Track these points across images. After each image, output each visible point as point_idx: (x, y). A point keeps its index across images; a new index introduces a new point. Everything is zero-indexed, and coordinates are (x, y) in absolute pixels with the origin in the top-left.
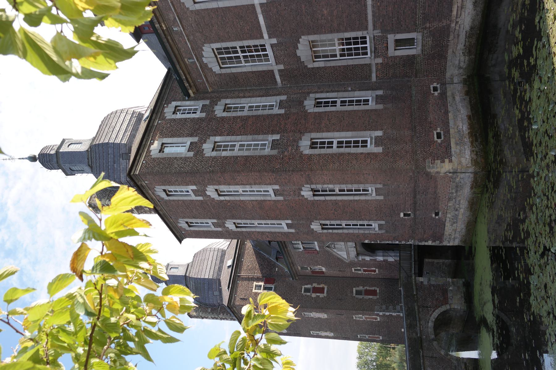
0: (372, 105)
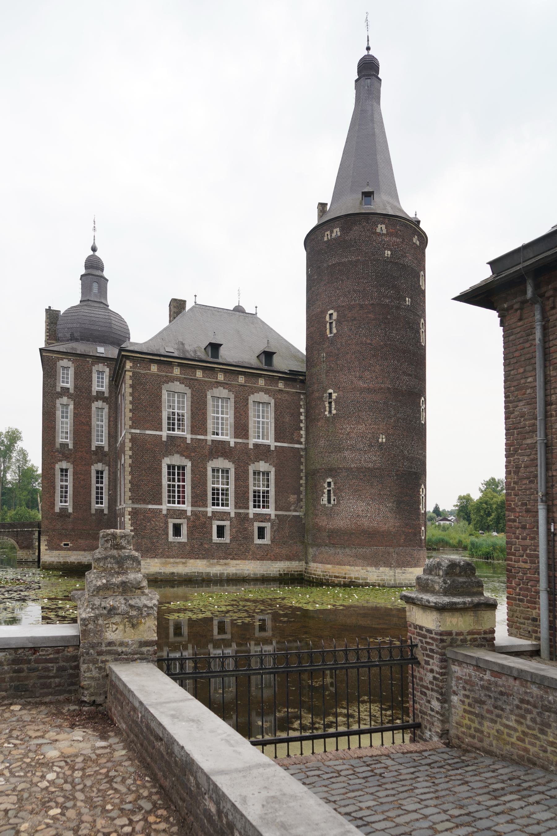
0: (95, 506)
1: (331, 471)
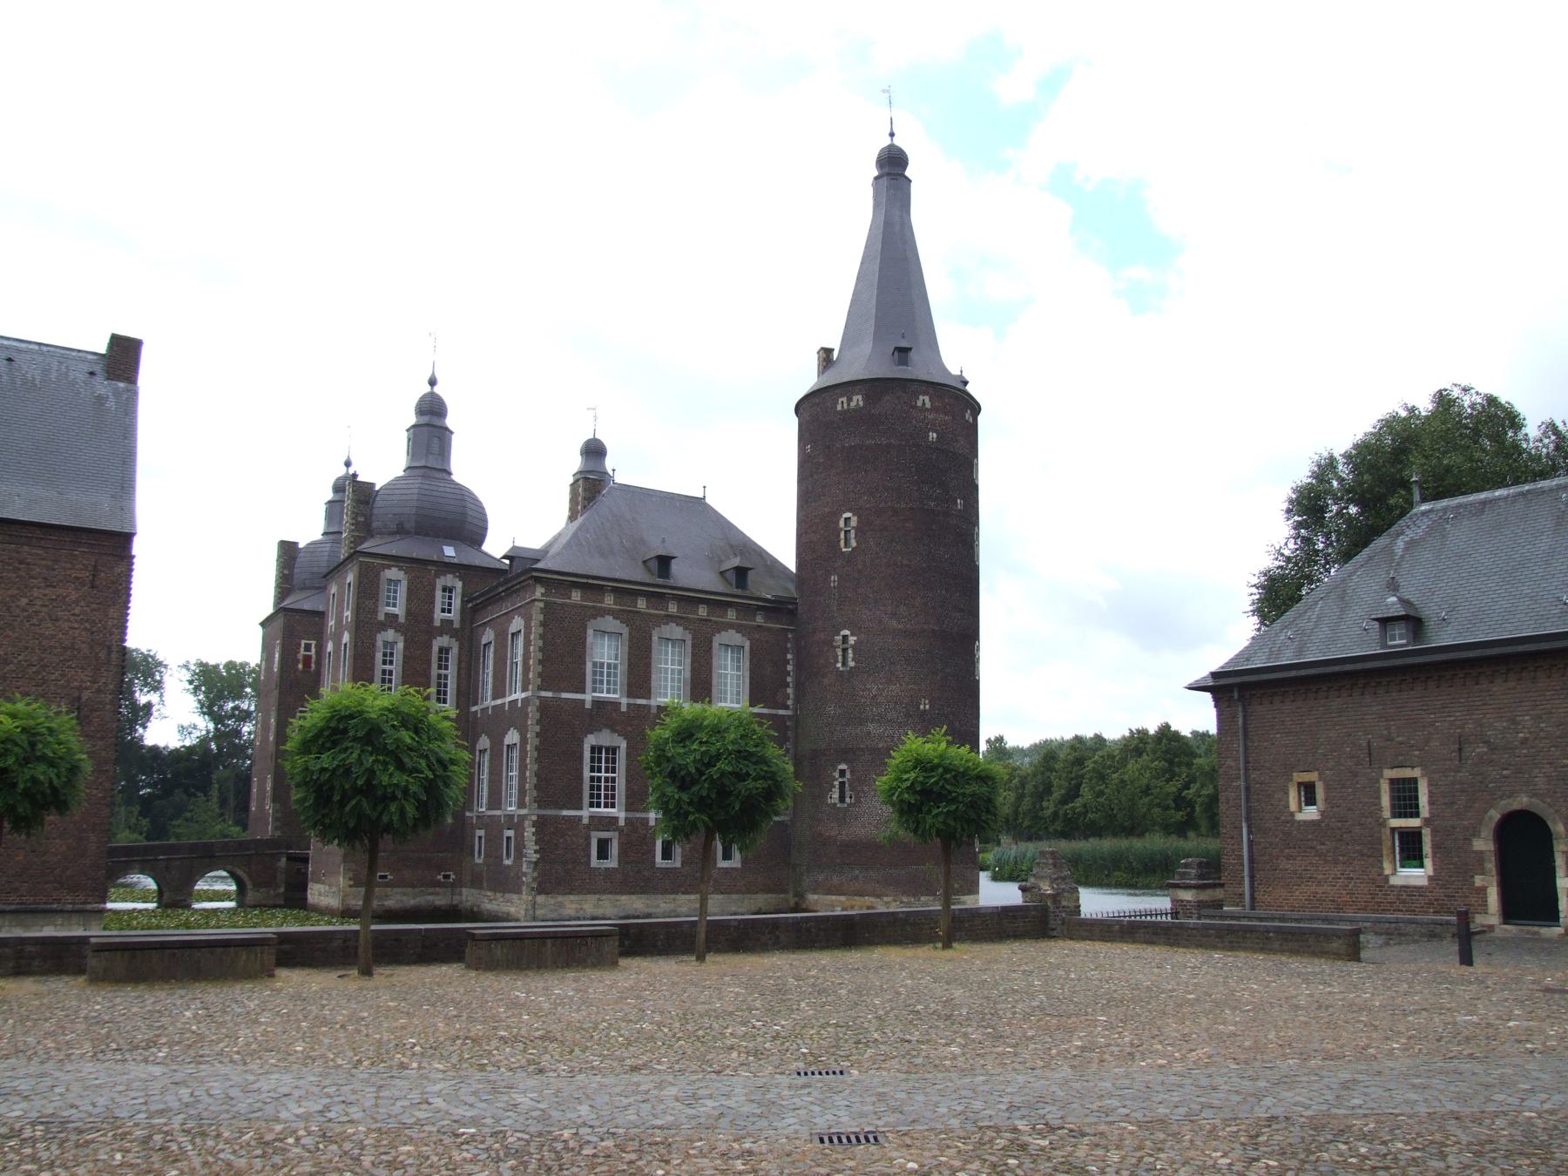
1: (846, 754)
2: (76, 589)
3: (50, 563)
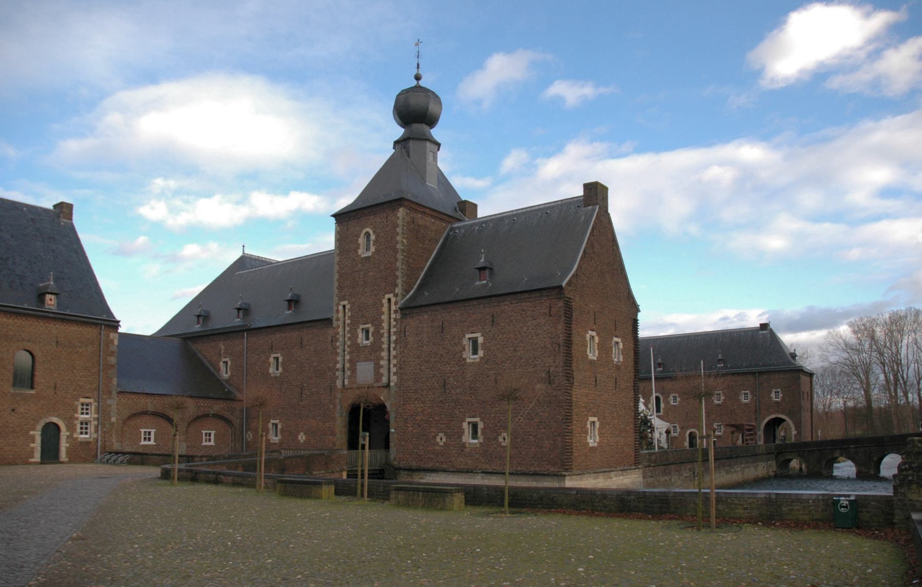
2: (544, 318)
3: (533, 309)
